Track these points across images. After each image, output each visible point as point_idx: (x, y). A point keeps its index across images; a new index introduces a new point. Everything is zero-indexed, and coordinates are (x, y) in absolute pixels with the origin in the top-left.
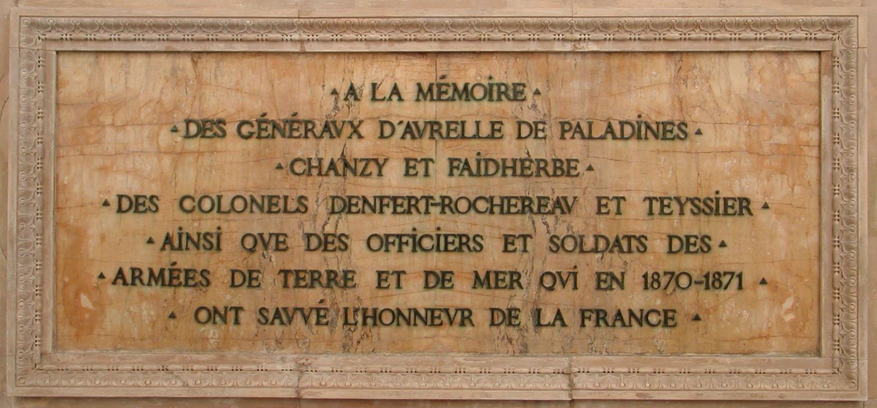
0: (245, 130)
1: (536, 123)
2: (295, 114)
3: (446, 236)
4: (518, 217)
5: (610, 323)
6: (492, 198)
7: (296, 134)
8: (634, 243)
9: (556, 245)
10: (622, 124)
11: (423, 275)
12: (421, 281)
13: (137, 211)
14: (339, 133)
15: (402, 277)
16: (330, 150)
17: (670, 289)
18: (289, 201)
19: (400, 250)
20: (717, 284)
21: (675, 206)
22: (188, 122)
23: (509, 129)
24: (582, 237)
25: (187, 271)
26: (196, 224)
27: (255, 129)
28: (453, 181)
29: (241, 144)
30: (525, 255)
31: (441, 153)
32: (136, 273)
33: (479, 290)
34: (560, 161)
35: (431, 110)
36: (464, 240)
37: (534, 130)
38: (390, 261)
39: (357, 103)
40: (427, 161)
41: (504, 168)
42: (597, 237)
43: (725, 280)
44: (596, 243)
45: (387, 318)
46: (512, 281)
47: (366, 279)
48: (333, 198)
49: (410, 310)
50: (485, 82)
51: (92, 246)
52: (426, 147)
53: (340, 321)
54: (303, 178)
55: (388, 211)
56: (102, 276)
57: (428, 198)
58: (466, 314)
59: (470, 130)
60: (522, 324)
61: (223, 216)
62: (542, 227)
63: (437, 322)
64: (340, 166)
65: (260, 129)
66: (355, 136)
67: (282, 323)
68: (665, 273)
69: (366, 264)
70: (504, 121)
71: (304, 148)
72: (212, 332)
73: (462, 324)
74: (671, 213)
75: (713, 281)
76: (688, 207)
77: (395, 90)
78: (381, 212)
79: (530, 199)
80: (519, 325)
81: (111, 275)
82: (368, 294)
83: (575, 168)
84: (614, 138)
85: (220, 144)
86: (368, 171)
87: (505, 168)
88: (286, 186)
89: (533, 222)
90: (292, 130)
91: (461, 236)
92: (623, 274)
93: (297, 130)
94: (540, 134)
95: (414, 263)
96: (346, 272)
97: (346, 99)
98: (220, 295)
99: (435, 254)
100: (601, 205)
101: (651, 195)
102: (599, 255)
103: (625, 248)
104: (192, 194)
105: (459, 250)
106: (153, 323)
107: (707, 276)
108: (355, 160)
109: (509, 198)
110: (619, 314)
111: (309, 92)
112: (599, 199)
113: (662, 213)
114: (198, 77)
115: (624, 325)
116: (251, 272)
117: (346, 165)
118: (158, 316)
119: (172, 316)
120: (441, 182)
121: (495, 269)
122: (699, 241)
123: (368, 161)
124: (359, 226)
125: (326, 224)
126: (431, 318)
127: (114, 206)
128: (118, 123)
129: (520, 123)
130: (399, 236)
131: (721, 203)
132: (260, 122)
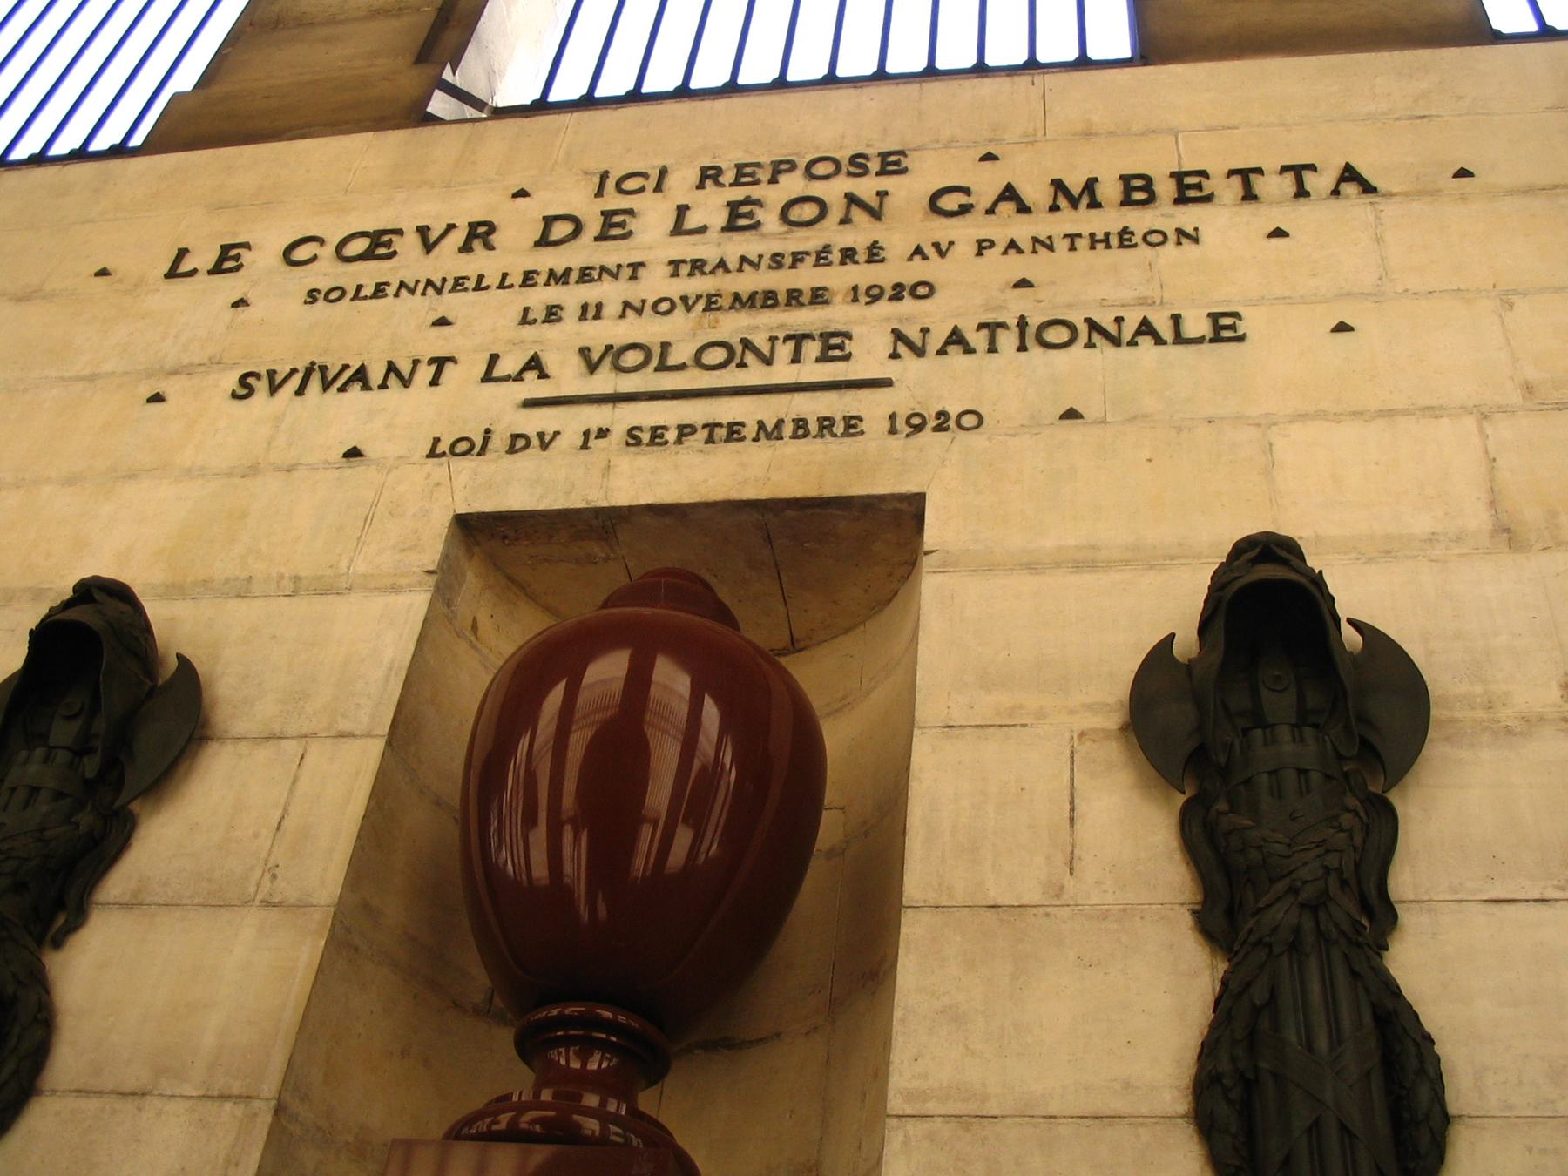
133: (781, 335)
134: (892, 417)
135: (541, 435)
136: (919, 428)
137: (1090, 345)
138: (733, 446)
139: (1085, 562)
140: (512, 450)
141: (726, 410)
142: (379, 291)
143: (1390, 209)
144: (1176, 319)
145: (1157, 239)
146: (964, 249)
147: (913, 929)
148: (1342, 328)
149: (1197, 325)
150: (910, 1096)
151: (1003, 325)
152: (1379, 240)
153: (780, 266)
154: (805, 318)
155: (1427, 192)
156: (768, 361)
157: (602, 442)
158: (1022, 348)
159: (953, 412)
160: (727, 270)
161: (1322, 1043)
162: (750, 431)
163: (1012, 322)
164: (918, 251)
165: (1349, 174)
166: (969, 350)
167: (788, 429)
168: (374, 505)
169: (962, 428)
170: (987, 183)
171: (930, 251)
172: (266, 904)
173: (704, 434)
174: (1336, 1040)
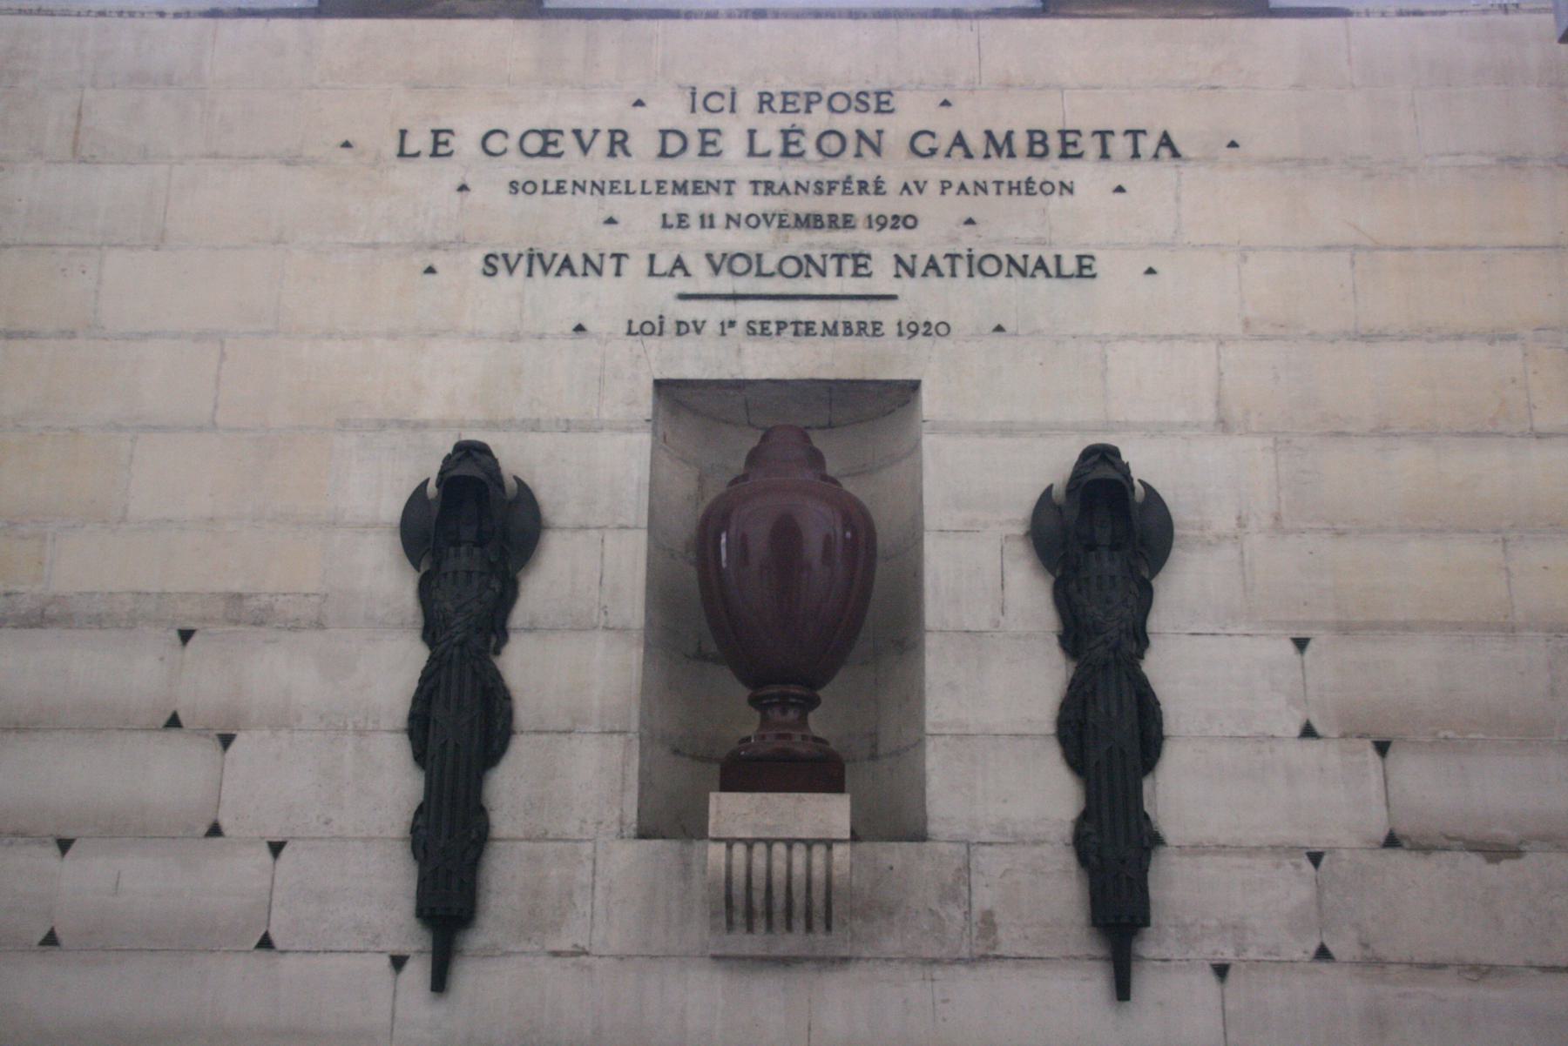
135: (695, 323)
136: (915, 333)
137: (1009, 275)
139: (1007, 430)
140: (679, 333)
141: (805, 311)
142: (559, 189)
144: (1058, 258)
145: (1047, 188)
146: (933, 188)
148: (1151, 271)
149: (1070, 266)
151: (959, 256)
152: (1178, 199)
154: (841, 239)
155: (1209, 160)
156: (823, 273)
158: (971, 275)
159: (934, 321)
160: (788, 193)
162: (818, 328)
163: (965, 253)
164: (906, 187)
165: (1166, 141)
166: (940, 274)
167: (840, 328)
171: (912, 187)
172: (606, 628)
173: (791, 329)
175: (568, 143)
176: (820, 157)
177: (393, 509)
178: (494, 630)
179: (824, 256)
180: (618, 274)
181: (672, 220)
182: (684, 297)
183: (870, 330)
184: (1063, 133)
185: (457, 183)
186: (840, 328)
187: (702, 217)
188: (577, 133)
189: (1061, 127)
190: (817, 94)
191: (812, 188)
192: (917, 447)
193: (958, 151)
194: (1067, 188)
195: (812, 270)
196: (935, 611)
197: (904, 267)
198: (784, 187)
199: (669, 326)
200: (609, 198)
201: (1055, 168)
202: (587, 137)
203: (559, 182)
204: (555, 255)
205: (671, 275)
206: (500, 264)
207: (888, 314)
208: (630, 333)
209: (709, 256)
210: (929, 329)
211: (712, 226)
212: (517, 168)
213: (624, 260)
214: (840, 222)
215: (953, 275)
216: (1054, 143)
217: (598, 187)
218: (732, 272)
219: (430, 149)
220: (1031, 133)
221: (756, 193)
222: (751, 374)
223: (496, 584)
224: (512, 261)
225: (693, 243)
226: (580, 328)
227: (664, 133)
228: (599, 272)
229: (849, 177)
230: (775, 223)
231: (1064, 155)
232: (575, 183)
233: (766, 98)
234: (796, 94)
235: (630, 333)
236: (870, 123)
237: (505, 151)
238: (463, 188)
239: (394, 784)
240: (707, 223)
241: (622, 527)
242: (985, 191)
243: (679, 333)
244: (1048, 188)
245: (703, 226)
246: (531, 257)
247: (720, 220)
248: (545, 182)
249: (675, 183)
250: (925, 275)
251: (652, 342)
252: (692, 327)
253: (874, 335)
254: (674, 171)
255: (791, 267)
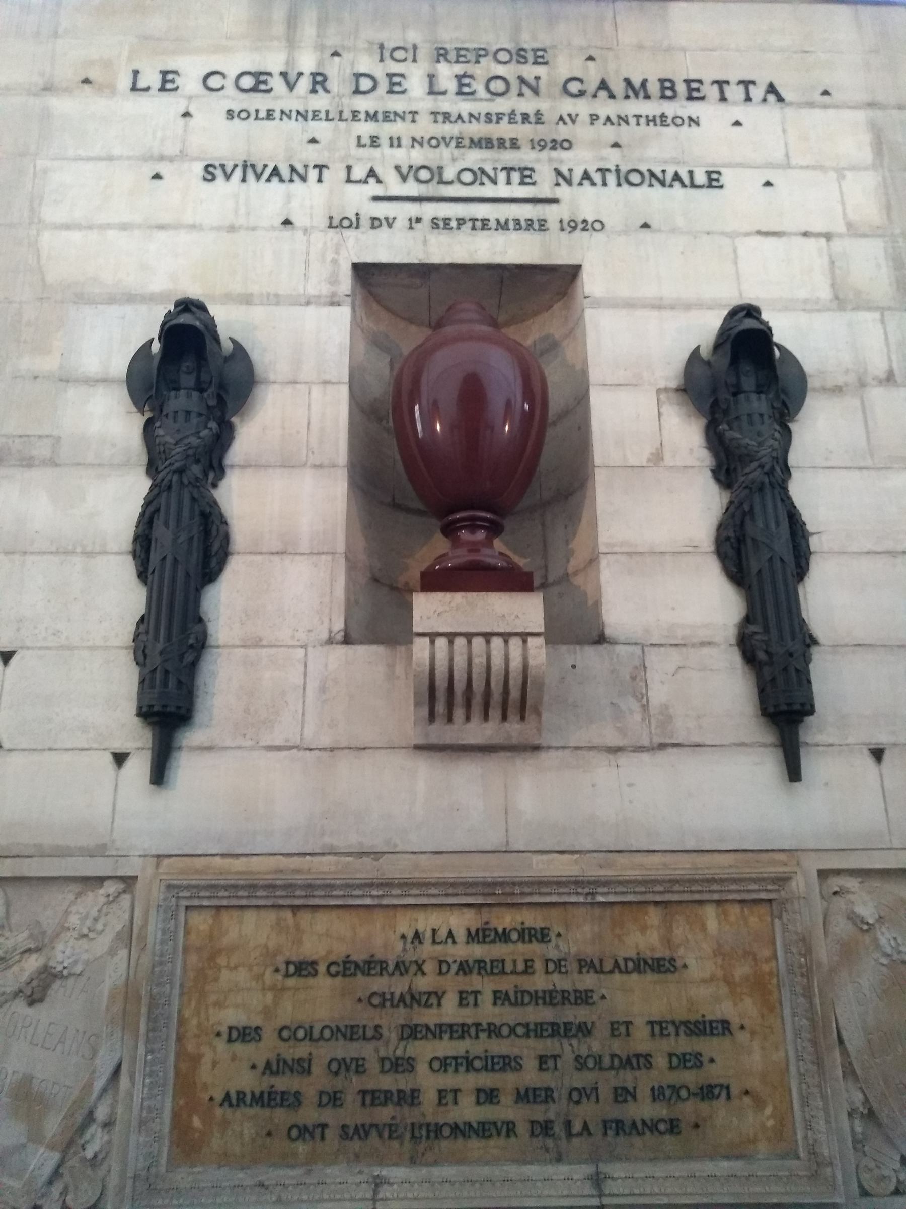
0: (333, 969)
1: (559, 960)
2: (373, 956)
3: (493, 1058)
4: (549, 1041)
5: (627, 1131)
6: (528, 1024)
7: (373, 972)
8: (642, 1060)
9: (581, 1063)
10: (626, 960)
11: (475, 1092)
12: (473, 1098)
13: (243, 1041)
14: (407, 971)
15: (458, 1094)
16: (399, 986)
17: (674, 1098)
18: (367, 1029)
19: (456, 1071)
20: (710, 1096)
21: (671, 1029)
22: (288, 963)
23: (538, 965)
24: (600, 1057)
25: (283, 1093)
26: (291, 1051)
27: (341, 968)
28: (497, 1010)
29: (329, 981)
30: (557, 1073)
31: (486, 986)
32: (241, 1095)
33: (520, 1105)
34: (581, 992)
35: (478, 951)
36: (507, 1061)
37: (558, 964)
38: (449, 1080)
39: (420, 946)
40: (476, 993)
41: (537, 998)
42: (613, 1056)
43: (716, 1091)
44: (612, 1062)
45: (446, 1132)
46: (546, 1097)
47: (429, 1097)
48: (403, 1026)
49: (465, 1123)
50: (519, 927)
51: (205, 1073)
52: (475, 982)
53: (408, 1136)
54: (378, 1009)
55: (446, 1036)
56: (211, 1099)
57: (477, 1025)
58: (511, 1126)
59: (509, 967)
60: (557, 1134)
61: (314, 1043)
62: (567, 1049)
63: (487, 1134)
64: (408, 999)
65: (345, 969)
66: (419, 973)
67: (360, 1138)
68: (669, 1086)
69: (429, 1082)
70: (535, 959)
71: (379, 984)
72: (302, 1148)
73: (508, 1136)
74: (669, 1035)
75: (707, 1092)
76: (682, 1028)
77: (450, 934)
78: (441, 1038)
79: (557, 1024)
80: (553, 1135)
81: (219, 1096)
82: (431, 1110)
83: (592, 997)
84: (621, 972)
85: (311, 981)
86: (430, 1002)
87: (537, 998)
88: (367, 1017)
89: (561, 1044)
90: (369, 969)
91: (504, 1057)
92: (635, 1088)
93: (374, 968)
94: (563, 970)
95: (468, 1081)
96: (413, 1091)
97: (412, 942)
98: (309, 1115)
99: (484, 1073)
100: (614, 1027)
101: (652, 1019)
102: (613, 1072)
103: (635, 1065)
104: (288, 1024)
105: (503, 1070)
106: (253, 1140)
107: (702, 1088)
108: (420, 993)
109: (541, 1024)
110: (634, 1124)
111: (383, 937)
112: (612, 1024)
113: (662, 1034)
114: (298, 927)
115: (639, 1134)
116: (335, 1093)
117: (413, 997)
118: (257, 1134)
119: (269, 1134)
120: (488, 1012)
121: (532, 1086)
122: (692, 1058)
123: (430, 994)
124: (424, 1050)
125: (396, 1048)
126: (484, 1130)
127: (225, 1036)
128: (232, 965)
129: (547, 961)
130: (455, 1058)
131: (707, 1025)
132: (345, 963)
133: (500, 167)
134: (561, 221)
136: (574, 228)
137: (651, 185)
138: (485, 232)
139: (658, 306)
142: (270, 115)
143: (789, 112)
144: (691, 173)
145: (678, 122)
147: (600, 476)
148: (768, 184)
149: (701, 179)
150: (608, 545)
151: (608, 170)
153: (490, 121)
154: (509, 157)
156: (495, 182)
157: (419, 226)
158: (619, 185)
159: (590, 219)
160: (463, 122)
161: (773, 526)
162: (493, 224)
163: (613, 168)
164: (561, 118)
165: (772, 89)
168: (308, 254)
169: (595, 230)
170: (593, 75)
171: (567, 119)
173: (470, 224)
174: (778, 524)
175: (277, 83)
176: (488, 96)
177: (120, 366)
178: (211, 467)
179: (495, 169)
180: (320, 180)
181: (366, 140)
182: (376, 199)
183: (536, 226)
184: (688, 82)
185: (182, 110)
186: (511, 225)
187: (391, 138)
188: (284, 74)
189: (686, 78)
190: (484, 49)
191: (483, 118)
192: (581, 318)
193: (603, 94)
194: (694, 121)
195: (485, 180)
196: (599, 456)
197: (562, 177)
198: (460, 117)
199: (365, 222)
200: (312, 124)
201: (682, 107)
202: (292, 77)
203: (268, 111)
204: (265, 166)
205: (366, 182)
206: (218, 172)
207: (551, 213)
208: (330, 226)
209: (397, 168)
210: (586, 225)
211: (399, 146)
212: (233, 100)
213: (325, 171)
214: (508, 144)
215: (605, 184)
216: (681, 88)
217: (302, 115)
218: (418, 180)
219: (158, 85)
220: (662, 81)
221: (436, 122)
222: (436, 259)
223: (213, 425)
224: (229, 170)
225: (387, 159)
226: (287, 222)
227: (358, 76)
228: (304, 179)
229: (513, 111)
230: (453, 144)
231: (690, 98)
232: (282, 112)
233: (442, 52)
234: (467, 50)
235: (330, 226)
236: (529, 71)
237: (223, 88)
238: (186, 115)
239: (119, 598)
240: (395, 142)
241: (326, 383)
242: (627, 123)
243: (373, 227)
244: (679, 121)
245: (391, 145)
246: (245, 167)
247: (406, 141)
248: (257, 111)
249: (367, 113)
250: (580, 184)
251: (350, 234)
252: (384, 222)
253: (540, 230)
254: (364, 104)
255: (467, 177)
